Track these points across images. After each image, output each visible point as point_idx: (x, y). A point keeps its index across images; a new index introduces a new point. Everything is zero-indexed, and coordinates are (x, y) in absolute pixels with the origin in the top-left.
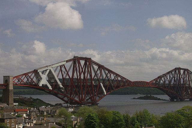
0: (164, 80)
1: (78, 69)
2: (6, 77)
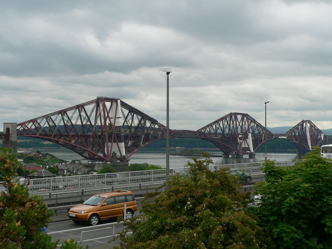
0: (216, 129)
1: (102, 113)
2: (7, 125)
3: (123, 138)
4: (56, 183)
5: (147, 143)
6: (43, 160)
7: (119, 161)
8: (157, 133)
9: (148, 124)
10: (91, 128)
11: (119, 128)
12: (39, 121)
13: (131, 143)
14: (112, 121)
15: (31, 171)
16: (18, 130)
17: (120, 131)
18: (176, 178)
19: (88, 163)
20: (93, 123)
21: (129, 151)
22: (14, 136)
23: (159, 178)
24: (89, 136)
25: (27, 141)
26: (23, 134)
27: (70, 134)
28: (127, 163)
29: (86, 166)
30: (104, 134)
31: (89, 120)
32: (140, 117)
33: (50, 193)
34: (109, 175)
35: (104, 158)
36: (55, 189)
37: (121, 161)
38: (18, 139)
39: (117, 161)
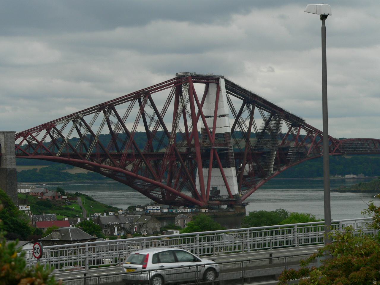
1: (188, 107)
3: (232, 159)
4: (96, 254)
5: (283, 169)
6: (70, 207)
7: (225, 207)
8: (305, 147)
9: (284, 128)
10: (166, 137)
11: (224, 138)
12: (59, 127)
13: (249, 167)
14: (210, 122)
15: (46, 230)
16: (17, 147)
17: (226, 144)
18: (346, 238)
19: (162, 212)
20: (170, 129)
21: (246, 186)
22: (11, 158)
23: (310, 240)
24: (163, 154)
25: (36, 169)
26: (28, 155)
27: (123, 151)
28: (243, 211)
29: (157, 218)
30: (192, 150)
31: (161, 122)
32: (267, 114)
33: (85, 275)
34: (206, 234)
35: (194, 200)
36: (95, 265)
37: (230, 206)
38: (18, 164)
39: (222, 207)
